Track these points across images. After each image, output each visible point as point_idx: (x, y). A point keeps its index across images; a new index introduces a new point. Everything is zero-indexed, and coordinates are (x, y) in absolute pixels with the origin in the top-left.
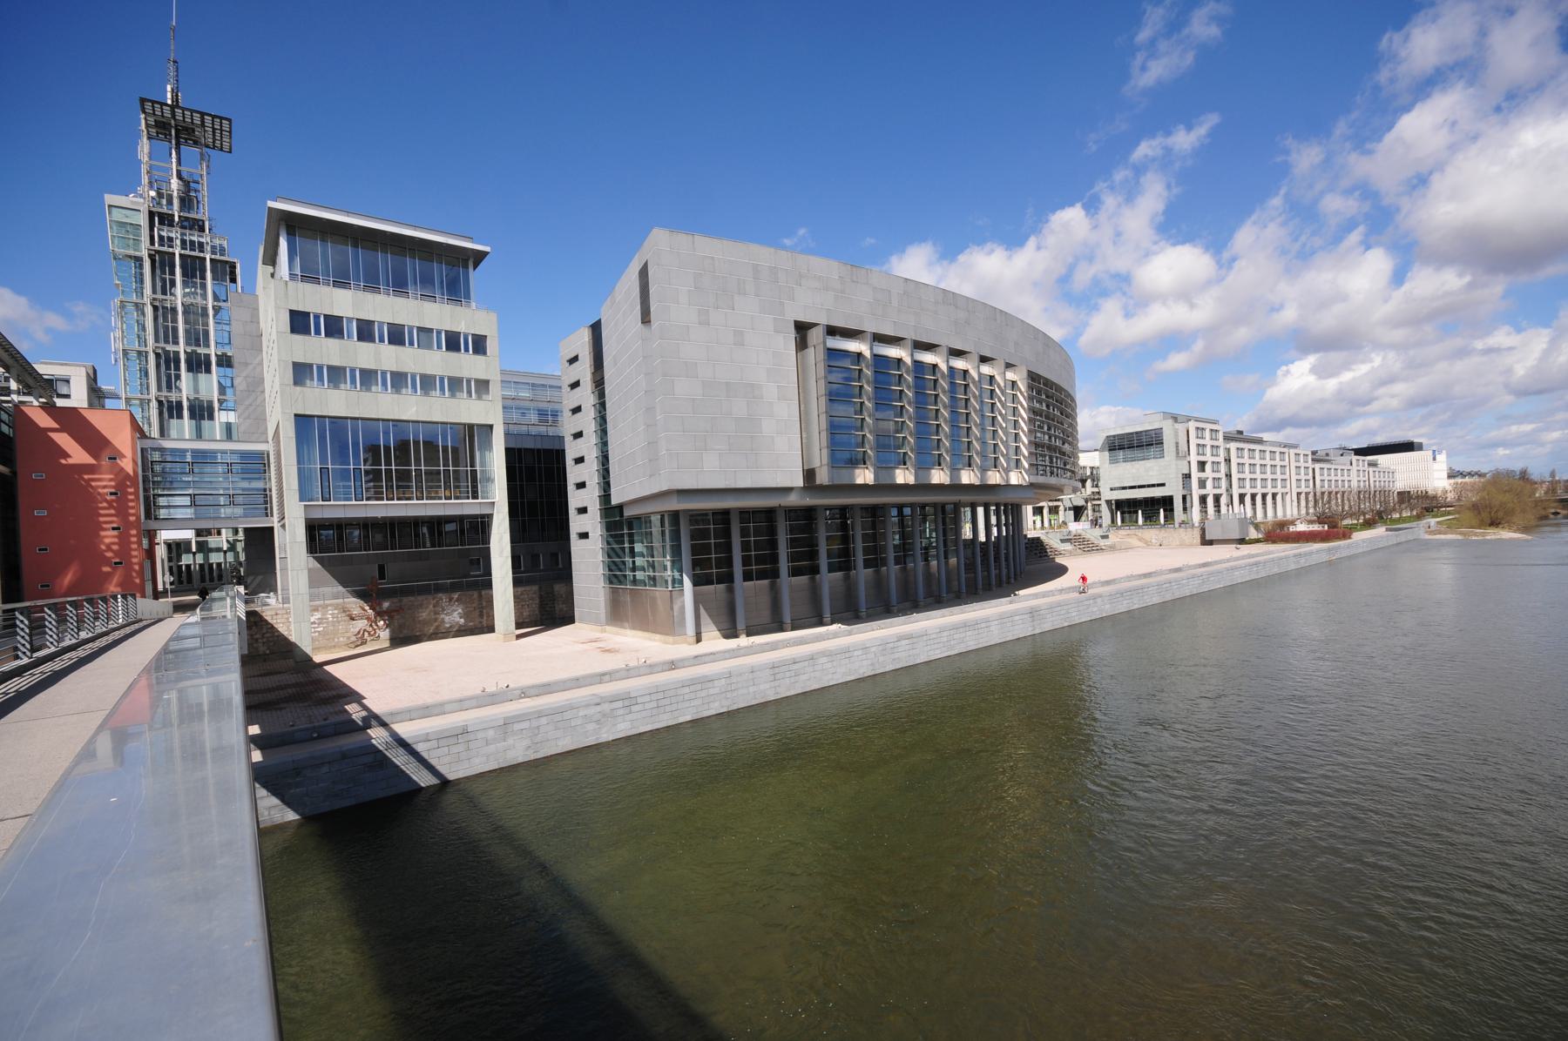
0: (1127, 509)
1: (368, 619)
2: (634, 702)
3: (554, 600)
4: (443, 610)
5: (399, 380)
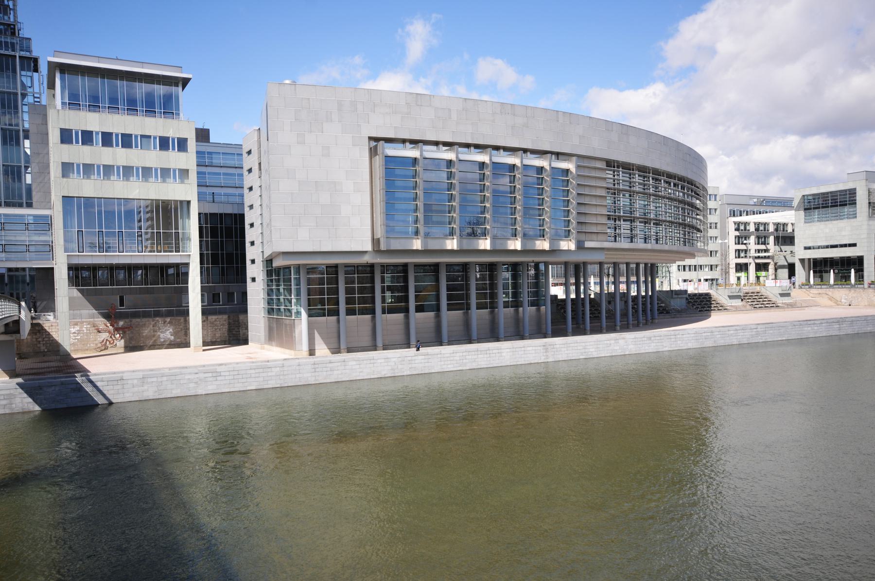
0: (820, 267)
1: (109, 332)
2: (219, 375)
3: (239, 326)
4: (160, 329)
5: (127, 171)
